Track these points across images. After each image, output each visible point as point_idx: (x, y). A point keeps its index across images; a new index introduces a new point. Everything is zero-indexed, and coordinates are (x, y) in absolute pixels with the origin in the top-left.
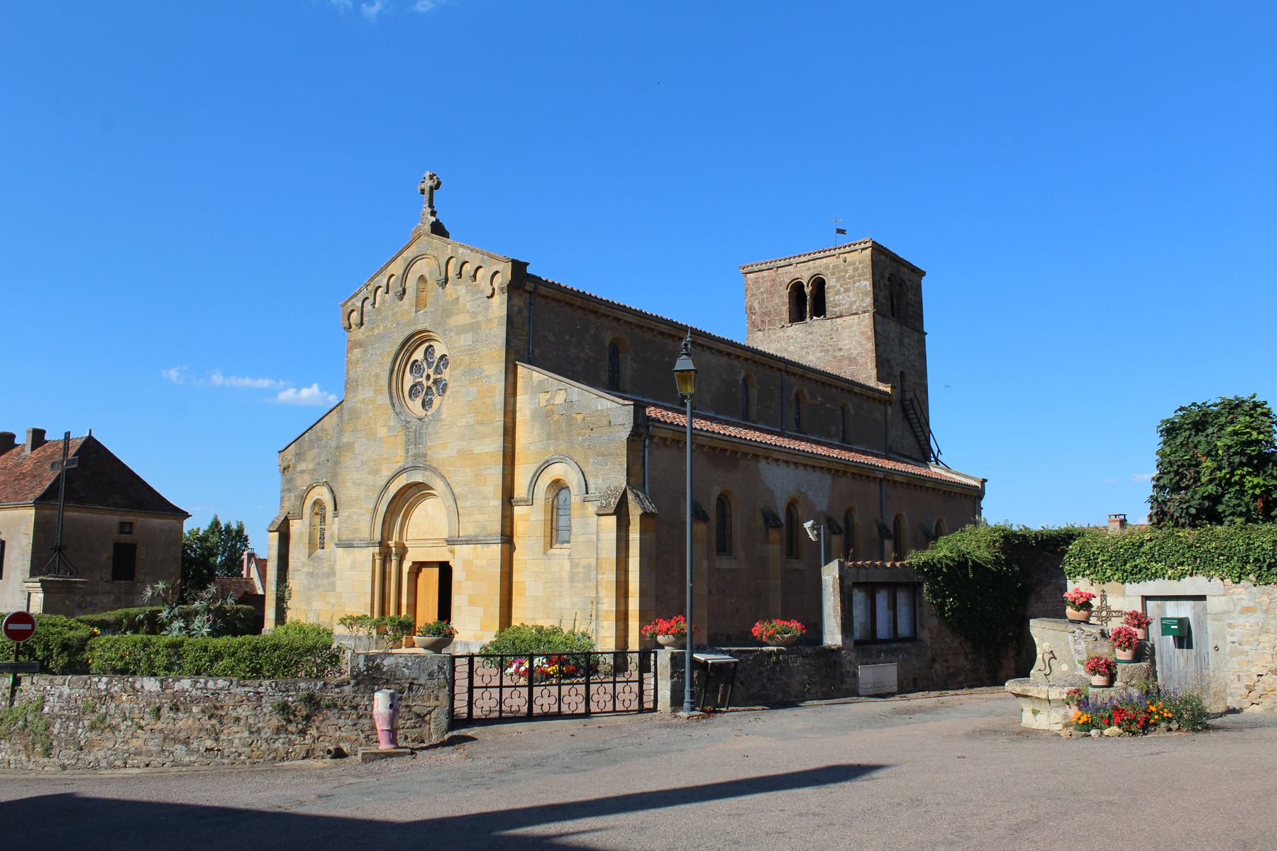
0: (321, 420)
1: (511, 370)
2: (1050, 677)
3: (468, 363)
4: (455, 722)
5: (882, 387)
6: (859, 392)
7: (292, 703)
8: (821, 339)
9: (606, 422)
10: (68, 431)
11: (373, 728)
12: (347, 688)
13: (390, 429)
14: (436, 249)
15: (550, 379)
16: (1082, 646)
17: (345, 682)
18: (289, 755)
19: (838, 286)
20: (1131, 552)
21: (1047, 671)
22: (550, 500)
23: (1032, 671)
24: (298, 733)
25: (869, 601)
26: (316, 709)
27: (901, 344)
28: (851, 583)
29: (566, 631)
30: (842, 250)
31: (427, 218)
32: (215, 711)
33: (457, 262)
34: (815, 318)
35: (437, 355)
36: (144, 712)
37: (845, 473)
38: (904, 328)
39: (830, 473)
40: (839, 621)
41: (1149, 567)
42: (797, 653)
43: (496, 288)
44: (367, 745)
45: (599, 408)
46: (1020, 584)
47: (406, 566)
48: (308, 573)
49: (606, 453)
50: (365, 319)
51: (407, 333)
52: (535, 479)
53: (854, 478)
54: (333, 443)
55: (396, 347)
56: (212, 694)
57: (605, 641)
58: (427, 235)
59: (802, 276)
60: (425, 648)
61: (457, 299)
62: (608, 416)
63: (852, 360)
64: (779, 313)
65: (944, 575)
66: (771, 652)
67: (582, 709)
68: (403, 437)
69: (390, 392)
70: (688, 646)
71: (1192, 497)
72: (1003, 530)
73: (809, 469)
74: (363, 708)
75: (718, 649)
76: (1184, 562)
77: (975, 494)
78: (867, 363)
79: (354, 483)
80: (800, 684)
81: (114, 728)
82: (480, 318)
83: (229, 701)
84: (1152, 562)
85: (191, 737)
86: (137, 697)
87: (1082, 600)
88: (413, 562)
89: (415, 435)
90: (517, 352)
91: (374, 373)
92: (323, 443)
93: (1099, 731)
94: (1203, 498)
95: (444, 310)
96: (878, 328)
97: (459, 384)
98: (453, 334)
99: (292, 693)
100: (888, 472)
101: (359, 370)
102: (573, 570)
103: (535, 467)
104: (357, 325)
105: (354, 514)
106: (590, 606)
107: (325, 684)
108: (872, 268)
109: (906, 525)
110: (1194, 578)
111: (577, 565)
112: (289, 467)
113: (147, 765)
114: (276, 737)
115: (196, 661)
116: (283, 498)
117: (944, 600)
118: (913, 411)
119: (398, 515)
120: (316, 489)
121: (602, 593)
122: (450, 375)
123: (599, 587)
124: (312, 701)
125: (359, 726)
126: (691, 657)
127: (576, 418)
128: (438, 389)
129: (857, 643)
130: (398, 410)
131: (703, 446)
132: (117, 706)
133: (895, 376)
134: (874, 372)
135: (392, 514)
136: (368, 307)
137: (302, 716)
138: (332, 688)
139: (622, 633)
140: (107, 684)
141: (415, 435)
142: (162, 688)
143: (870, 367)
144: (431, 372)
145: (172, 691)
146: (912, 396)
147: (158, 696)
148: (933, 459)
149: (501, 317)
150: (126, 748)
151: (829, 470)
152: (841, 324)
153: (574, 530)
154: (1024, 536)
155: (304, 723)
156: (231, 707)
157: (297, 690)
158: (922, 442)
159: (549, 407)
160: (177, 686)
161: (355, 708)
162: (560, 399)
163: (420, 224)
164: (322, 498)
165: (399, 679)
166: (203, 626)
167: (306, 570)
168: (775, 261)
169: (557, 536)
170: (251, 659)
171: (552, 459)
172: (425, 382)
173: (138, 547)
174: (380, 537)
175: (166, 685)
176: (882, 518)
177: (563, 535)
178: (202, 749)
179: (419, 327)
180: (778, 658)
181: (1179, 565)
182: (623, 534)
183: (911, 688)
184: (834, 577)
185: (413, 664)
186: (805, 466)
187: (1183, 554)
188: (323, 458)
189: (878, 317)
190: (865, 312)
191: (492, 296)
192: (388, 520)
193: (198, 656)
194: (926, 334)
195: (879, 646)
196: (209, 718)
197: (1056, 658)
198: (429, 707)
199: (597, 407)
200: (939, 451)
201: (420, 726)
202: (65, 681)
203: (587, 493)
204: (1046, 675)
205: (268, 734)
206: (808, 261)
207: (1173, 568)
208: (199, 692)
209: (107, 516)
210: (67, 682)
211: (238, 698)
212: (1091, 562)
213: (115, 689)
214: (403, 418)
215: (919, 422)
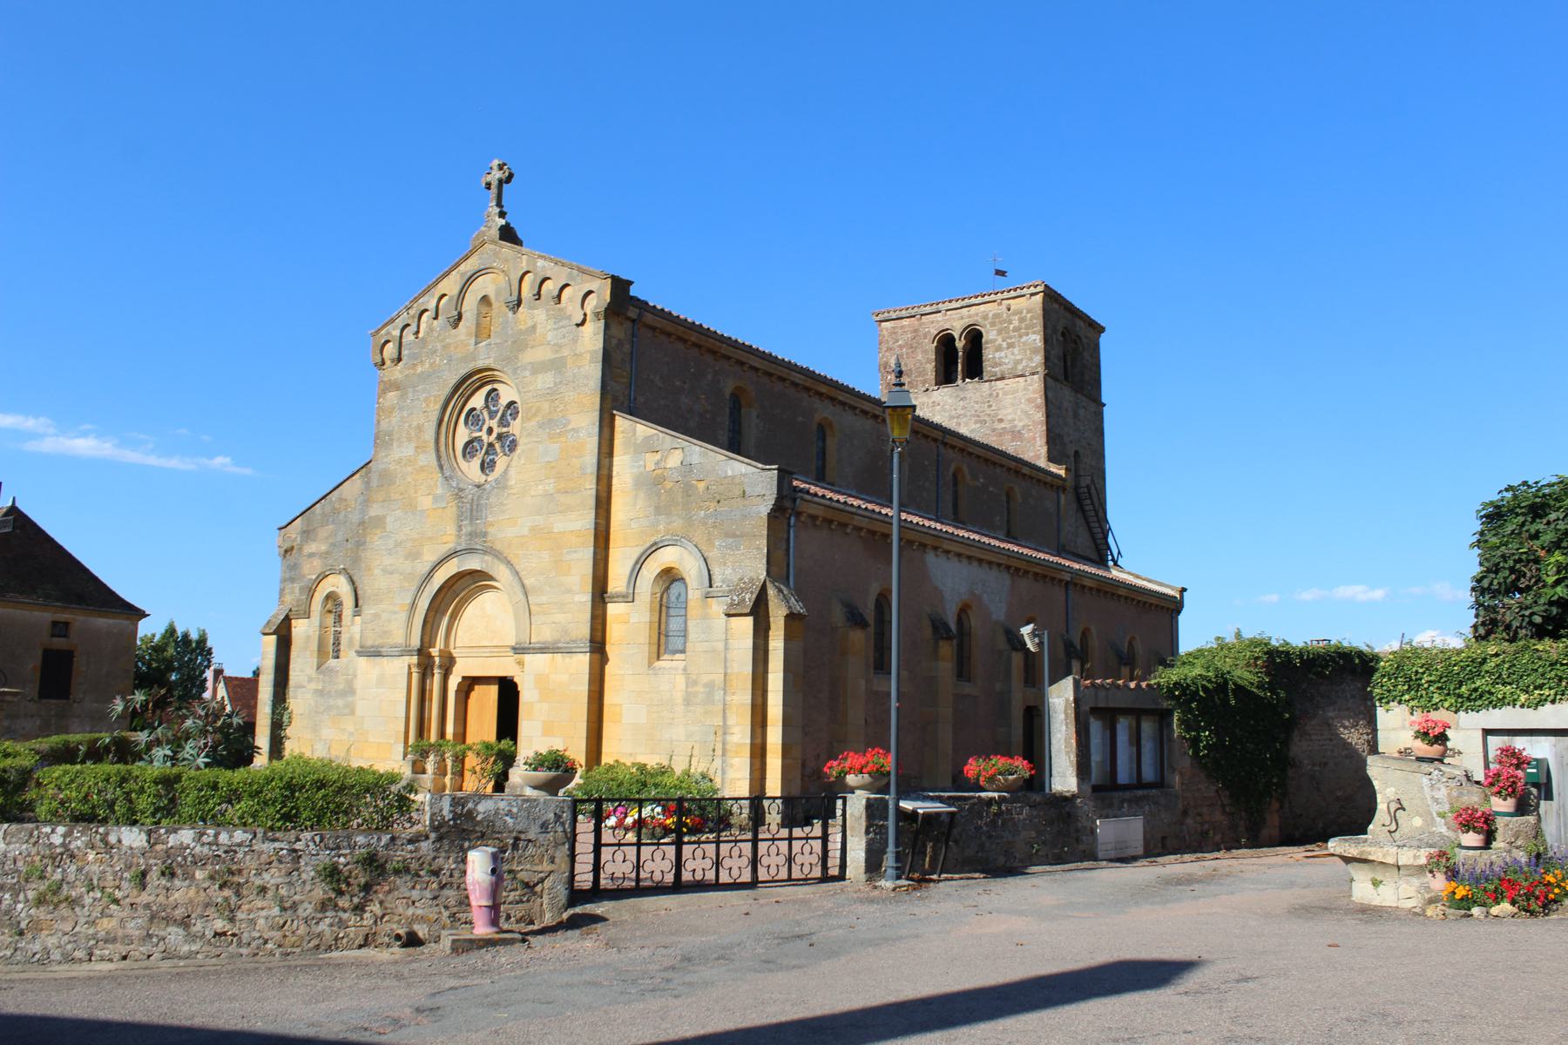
1: (606, 422)
2: (1396, 835)
4: (576, 896)
5: (1054, 468)
6: (1027, 472)
7: (345, 866)
8: (977, 407)
9: (738, 492)
11: (465, 902)
12: (425, 846)
13: (436, 499)
14: (506, 261)
16: (1442, 793)
17: (421, 836)
18: (339, 942)
20: (1470, 671)
21: (1393, 827)
22: (658, 595)
23: (1371, 827)
24: (353, 910)
25: (1108, 732)
26: (379, 875)
27: (1076, 416)
28: (1087, 708)
29: (678, 770)
30: (1006, 295)
31: (494, 221)
32: (228, 877)
33: (535, 279)
34: (967, 380)
35: (504, 401)
36: (121, 879)
37: (1026, 572)
38: (1079, 396)
39: (1009, 573)
40: (1073, 758)
41: (1493, 690)
42: (1022, 802)
43: (588, 313)
44: (452, 928)
45: (730, 473)
46: (1287, 715)
47: (454, 682)
48: (316, 691)
49: (738, 533)
50: (405, 352)
51: (463, 372)
52: (638, 566)
53: (1036, 580)
55: (447, 390)
56: (226, 852)
57: (735, 783)
58: (493, 242)
60: (535, 788)
61: (534, 327)
63: (1016, 435)
64: (922, 373)
65: (1200, 700)
66: (992, 799)
67: (746, 877)
68: (454, 509)
70: (893, 788)
71: (1536, 602)
72: (1266, 644)
73: (985, 566)
74: (448, 874)
75: (925, 794)
76: (1544, 684)
77: (1172, 607)
78: (1035, 438)
79: (383, 570)
80: (1026, 844)
81: (73, 903)
82: (565, 352)
83: (250, 863)
84: (1498, 684)
85: (193, 916)
86: (111, 857)
87: (1437, 731)
88: (464, 678)
89: (472, 506)
90: (615, 399)
91: (415, 424)
92: (341, 517)
93: (1484, 909)
94: (1551, 603)
95: (515, 342)
96: (1049, 395)
98: (527, 373)
99: (343, 852)
100: (1077, 574)
101: (394, 420)
103: (639, 550)
104: (393, 361)
106: (712, 737)
107: (393, 839)
108: (1044, 318)
109: (1095, 643)
110: (1557, 705)
111: (695, 683)
112: (292, 548)
113: (125, 958)
114: (319, 916)
115: (200, 803)
117: (1198, 733)
118: (1088, 502)
119: (444, 613)
121: (731, 721)
122: (522, 428)
124: (373, 863)
125: (441, 900)
126: (897, 805)
128: (503, 447)
129: (1096, 789)
130: (448, 474)
131: (861, 529)
132: (79, 870)
133: (1068, 457)
134: (1044, 450)
135: (436, 612)
136: (409, 336)
137: (359, 885)
138: (402, 845)
139: (757, 774)
140: (65, 836)
143: (1039, 443)
144: (494, 423)
145: (164, 847)
146: (1089, 482)
148: (1111, 563)
149: (595, 351)
150: (91, 931)
151: (1008, 568)
153: (692, 636)
154: (1287, 653)
155: (362, 895)
156: (254, 872)
157: (352, 847)
158: (1099, 541)
159: (659, 471)
160: (173, 840)
161: (436, 873)
162: (674, 460)
163: (483, 228)
164: (337, 590)
165: (499, 833)
166: (199, 756)
167: (313, 686)
168: (919, 307)
169: (666, 643)
170: (283, 802)
171: (662, 541)
172: (485, 437)
173: (75, 654)
176: (1067, 631)
177: (676, 642)
178: (209, 934)
179: (480, 364)
180: (1000, 808)
181: (1536, 688)
182: (761, 642)
183: (1160, 850)
184: (1067, 700)
185: (519, 810)
186: (980, 561)
187: (1543, 675)
188: (340, 537)
189: (1049, 379)
190: (1033, 374)
191: (582, 323)
192: (430, 620)
193: (203, 796)
194: (1104, 405)
195: (1121, 794)
196: (221, 887)
197: (1404, 810)
198: (541, 872)
199: (726, 472)
200: (1119, 553)
201: (528, 901)
203: (711, 586)
204: (1390, 832)
205: (308, 912)
206: (962, 308)
207: (1527, 692)
208: (206, 849)
209: (35, 613)
211: (264, 858)
212: (1411, 683)
213: (78, 843)
214: (454, 484)
215: (1097, 515)
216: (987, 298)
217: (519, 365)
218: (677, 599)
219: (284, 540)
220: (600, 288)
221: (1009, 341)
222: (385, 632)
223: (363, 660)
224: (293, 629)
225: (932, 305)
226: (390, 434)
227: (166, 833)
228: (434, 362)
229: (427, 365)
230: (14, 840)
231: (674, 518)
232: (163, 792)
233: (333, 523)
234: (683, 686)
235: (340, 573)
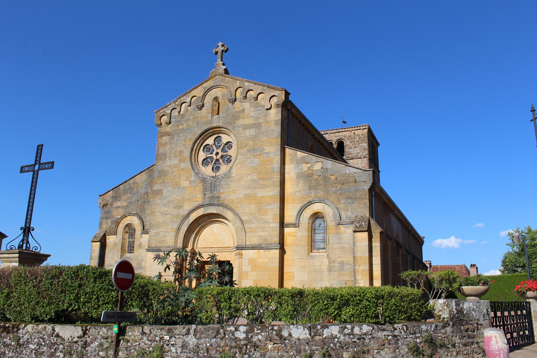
0: (133, 177)
3: (252, 144)
10: (40, 144)
13: (191, 182)
15: (310, 156)
19: (351, 145)
22: (311, 224)
30: (354, 129)
33: (243, 91)
43: (273, 105)
45: (348, 172)
50: (173, 120)
51: (205, 128)
52: (301, 212)
54: (143, 191)
55: (196, 136)
56: (359, 339)
58: (221, 75)
59: (332, 139)
61: (243, 110)
62: (354, 176)
68: (201, 187)
86: (286, 346)
89: (211, 185)
91: (178, 150)
92: (135, 190)
95: (233, 116)
98: (240, 129)
101: (167, 149)
102: (331, 265)
111: (334, 262)
112: (107, 204)
116: (102, 222)
120: (129, 218)
123: (356, 273)
127: (330, 178)
135: (189, 232)
140: (247, 332)
141: (211, 185)
142: (310, 335)
144: (219, 151)
145: (321, 337)
147: (307, 343)
149: (277, 120)
152: (352, 163)
156: (376, 351)
159: (310, 171)
160: (326, 333)
162: (318, 167)
164: (132, 223)
171: (313, 201)
172: (215, 157)
174: (181, 246)
175: (315, 332)
179: (214, 125)
188: (134, 199)
190: (365, 158)
199: (346, 172)
202: (189, 330)
203: (341, 220)
208: (347, 338)
210: (192, 332)
213: (259, 337)
216: (346, 130)
217: (236, 125)
218: (319, 226)
219: (102, 201)
220: (279, 94)
221: (355, 145)
222: (162, 241)
224: (107, 240)
225: (324, 131)
226: (165, 154)
227: (321, 329)
228: (189, 124)
230: (203, 336)
231: (319, 191)
232: (391, 295)
233: (130, 193)
234: (327, 263)
235: (134, 215)
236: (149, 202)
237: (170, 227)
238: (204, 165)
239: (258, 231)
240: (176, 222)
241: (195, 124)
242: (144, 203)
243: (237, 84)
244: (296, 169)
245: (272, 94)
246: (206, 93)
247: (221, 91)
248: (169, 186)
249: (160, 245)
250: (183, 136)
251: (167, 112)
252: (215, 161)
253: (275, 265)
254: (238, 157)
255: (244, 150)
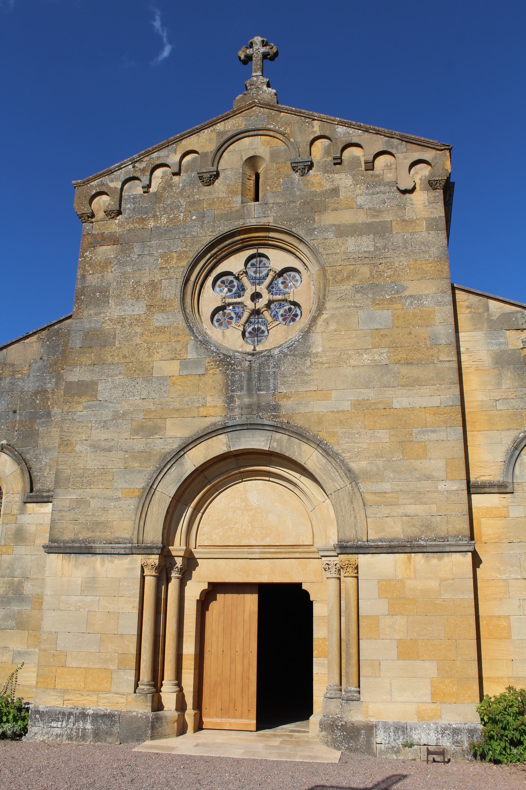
3: (368, 275)
13: (185, 364)
43: (418, 182)
50: (127, 206)
51: (224, 228)
55: (199, 247)
61: (335, 191)
68: (220, 377)
69: (184, 309)
82: (388, 217)
91: (146, 280)
95: (306, 203)
97: (348, 304)
105: (93, 498)
144: (262, 289)
179: (252, 222)
217: (315, 226)
220: (435, 158)
222: (97, 524)
223: (56, 560)
229: (164, 220)
236: (49, 415)
237: (120, 486)
238: (216, 324)
239: (405, 501)
240: (140, 472)
241: (194, 218)
242: (33, 417)
243: (315, 129)
244: (488, 343)
245: (417, 156)
246: (226, 145)
247: (268, 143)
248: (117, 372)
249: (90, 535)
250: (159, 246)
251: (112, 185)
252: (251, 314)
253: (461, 596)
254: (328, 305)
255: (346, 287)
